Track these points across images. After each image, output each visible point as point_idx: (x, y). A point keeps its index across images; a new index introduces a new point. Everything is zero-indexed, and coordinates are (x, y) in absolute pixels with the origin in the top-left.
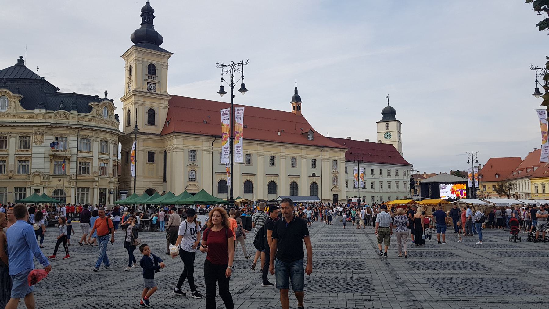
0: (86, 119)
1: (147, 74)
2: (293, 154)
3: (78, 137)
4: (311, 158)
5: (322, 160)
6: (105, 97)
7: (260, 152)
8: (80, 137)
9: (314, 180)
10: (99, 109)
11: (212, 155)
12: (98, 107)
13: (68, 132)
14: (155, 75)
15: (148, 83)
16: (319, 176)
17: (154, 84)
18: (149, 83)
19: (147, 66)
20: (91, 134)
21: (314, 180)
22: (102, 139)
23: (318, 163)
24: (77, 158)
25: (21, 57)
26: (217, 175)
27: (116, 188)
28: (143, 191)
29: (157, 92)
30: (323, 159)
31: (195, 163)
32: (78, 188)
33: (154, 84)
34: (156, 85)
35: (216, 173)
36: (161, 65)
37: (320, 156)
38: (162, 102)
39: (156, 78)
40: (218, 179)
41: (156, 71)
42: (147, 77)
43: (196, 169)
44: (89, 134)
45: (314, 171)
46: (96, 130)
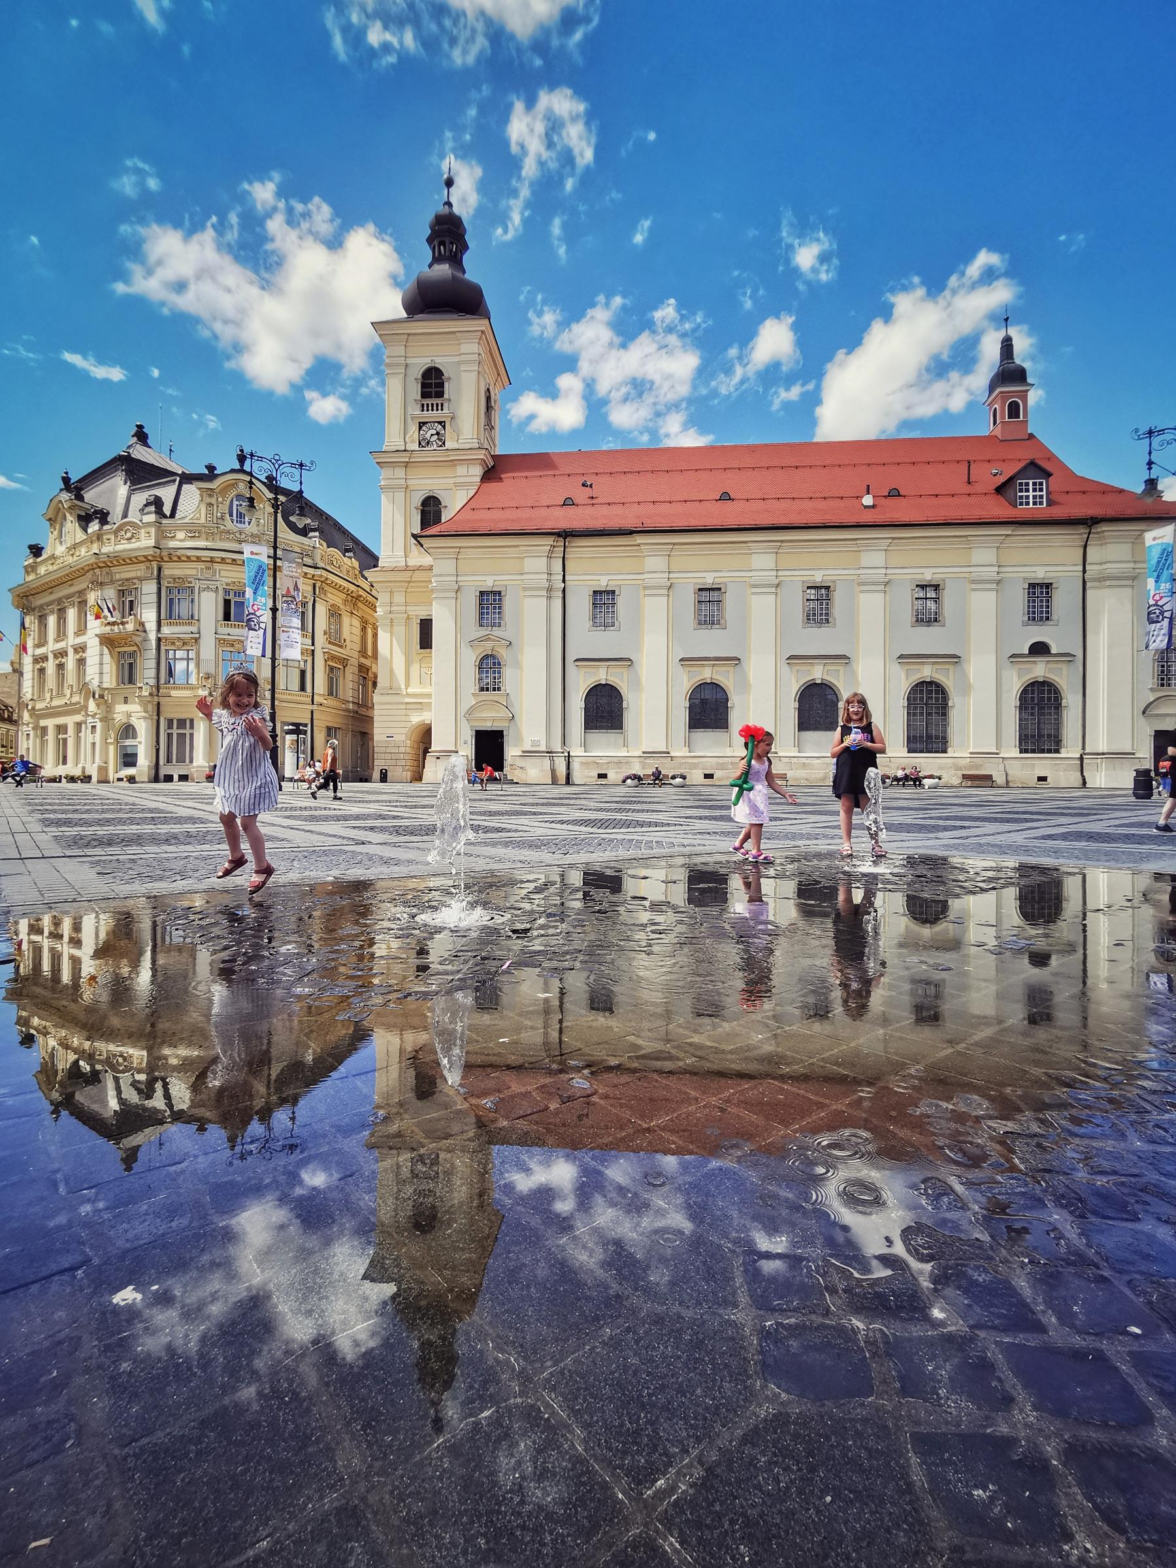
0: (181, 535)
1: (419, 397)
2: (922, 570)
3: (159, 583)
4: (1025, 579)
5: (1088, 585)
6: (238, 467)
7: (757, 577)
8: (165, 583)
9: (1040, 669)
10: (213, 501)
11: (559, 602)
12: (210, 496)
13: (139, 574)
14: (440, 394)
15: (421, 425)
16: (1068, 655)
17: (440, 423)
18: (424, 423)
19: (420, 376)
20: (194, 572)
21: (1040, 669)
22: (227, 584)
23: (1064, 601)
24: (159, 640)
25: (140, 427)
26: (582, 671)
27: (309, 722)
28: (405, 731)
29: (449, 445)
30: (1094, 580)
31: (496, 632)
32: (170, 722)
33: (440, 423)
34: (444, 427)
35: (577, 660)
36: (459, 363)
37: (1081, 568)
38: (461, 470)
39: (445, 405)
40: (581, 683)
41: (446, 385)
42: (419, 407)
43: (503, 653)
44: (188, 572)
45: (1038, 634)
46: (199, 560)
